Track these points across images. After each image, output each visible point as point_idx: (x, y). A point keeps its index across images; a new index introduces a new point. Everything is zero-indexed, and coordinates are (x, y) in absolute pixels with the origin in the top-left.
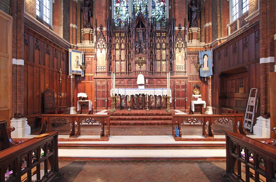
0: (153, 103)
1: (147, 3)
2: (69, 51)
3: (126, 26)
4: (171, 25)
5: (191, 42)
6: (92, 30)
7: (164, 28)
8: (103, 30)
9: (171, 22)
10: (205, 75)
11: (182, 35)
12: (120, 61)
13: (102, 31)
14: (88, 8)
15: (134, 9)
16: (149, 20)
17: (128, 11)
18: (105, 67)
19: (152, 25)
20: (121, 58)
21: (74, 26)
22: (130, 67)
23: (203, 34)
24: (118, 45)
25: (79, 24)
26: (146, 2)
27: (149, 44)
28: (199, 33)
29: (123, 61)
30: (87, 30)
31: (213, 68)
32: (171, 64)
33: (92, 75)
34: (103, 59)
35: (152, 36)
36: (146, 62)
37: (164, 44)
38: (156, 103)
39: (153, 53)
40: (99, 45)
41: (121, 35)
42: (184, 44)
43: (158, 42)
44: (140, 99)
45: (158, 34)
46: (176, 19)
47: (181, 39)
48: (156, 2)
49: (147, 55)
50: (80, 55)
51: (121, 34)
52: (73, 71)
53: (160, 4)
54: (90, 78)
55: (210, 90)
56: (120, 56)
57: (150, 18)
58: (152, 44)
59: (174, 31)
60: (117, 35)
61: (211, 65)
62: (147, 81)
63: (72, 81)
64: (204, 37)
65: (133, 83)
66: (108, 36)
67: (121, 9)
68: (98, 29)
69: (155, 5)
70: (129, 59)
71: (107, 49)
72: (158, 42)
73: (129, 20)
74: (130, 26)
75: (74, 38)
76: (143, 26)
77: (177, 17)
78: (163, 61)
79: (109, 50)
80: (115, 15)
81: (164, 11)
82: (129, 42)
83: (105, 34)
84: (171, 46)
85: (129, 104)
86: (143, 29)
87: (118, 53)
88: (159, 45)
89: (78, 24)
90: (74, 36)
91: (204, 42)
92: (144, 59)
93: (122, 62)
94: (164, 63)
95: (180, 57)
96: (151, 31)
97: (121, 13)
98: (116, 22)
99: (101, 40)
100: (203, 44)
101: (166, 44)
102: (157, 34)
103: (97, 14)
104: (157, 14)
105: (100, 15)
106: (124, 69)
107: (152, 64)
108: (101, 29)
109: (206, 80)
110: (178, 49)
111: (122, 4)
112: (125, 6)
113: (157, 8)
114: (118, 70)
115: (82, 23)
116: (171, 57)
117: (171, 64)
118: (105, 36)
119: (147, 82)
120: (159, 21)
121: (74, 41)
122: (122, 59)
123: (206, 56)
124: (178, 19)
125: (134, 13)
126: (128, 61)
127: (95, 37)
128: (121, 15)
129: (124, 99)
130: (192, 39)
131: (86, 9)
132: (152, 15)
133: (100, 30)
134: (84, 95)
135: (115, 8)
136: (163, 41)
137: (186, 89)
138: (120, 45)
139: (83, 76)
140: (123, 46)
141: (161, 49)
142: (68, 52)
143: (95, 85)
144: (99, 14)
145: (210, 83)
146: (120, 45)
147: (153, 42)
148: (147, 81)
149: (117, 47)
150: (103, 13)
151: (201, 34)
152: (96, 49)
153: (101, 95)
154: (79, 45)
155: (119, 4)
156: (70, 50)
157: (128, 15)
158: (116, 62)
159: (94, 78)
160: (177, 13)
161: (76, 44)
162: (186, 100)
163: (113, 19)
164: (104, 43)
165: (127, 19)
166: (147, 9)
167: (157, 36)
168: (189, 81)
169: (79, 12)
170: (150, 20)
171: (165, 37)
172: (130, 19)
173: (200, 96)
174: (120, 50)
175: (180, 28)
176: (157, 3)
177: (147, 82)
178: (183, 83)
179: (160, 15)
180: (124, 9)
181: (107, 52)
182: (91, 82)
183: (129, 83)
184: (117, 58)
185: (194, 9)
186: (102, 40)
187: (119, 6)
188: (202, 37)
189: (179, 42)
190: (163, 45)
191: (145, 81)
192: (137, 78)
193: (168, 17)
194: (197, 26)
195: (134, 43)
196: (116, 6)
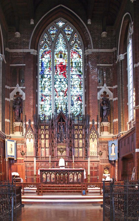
1: (67, 101)
2: (6, 140)
3: (49, 120)
4: (86, 120)
5: (103, 133)
6: (22, 123)
7: (81, 122)
8: (31, 124)
9: (86, 118)
10: (113, 159)
11: (94, 128)
12: (45, 148)
13: (30, 125)
14: (19, 106)
15: (56, 106)
16: (68, 116)
17: (51, 108)
18: (33, 153)
19: (71, 120)
20: (45, 146)
21: (8, 121)
22: (53, 153)
23: (112, 127)
24: (43, 135)
25: (11, 119)
26: (66, 101)
27: (68, 135)
28: (109, 126)
29: (48, 148)
30: (18, 124)
31: (118, 154)
32: (86, 150)
33: (23, 158)
34: (31, 147)
35: (71, 128)
36: (66, 149)
37: (81, 135)
38: (73, 179)
39: (72, 142)
40: (28, 136)
41: (46, 127)
42: (96, 136)
43: (76, 133)
44: (62, 177)
45: (76, 127)
46: (90, 116)
47: (94, 131)
48: (74, 101)
49: (67, 144)
50: (13, 143)
51: (46, 127)
52: (8, 156)
53: (78, 103)
54: (21, 161)
55: (116, 170)
56: (45, 144)
57: (69, 114)
58: (71, 135)
59: (88, 125)
60: (43, 127)
61: (117, 151)
62: (67, 163)
63: (7, 163)
64: (112, 130)
65: (55, 165)
66: (35, 128)
67: (45, 107)
68: (27, 123)
69: (73, 103)
70: (52, 147)
71: (34, 139)
72: (76, 133)
73: (52, 115)
74: (53, 120)
75: (8, 130)
76: (63, 121)
77: (91, 114)
78: (80, 148)
79: (36, 140)
80: (40, 111)
81: (81, 108)
82: (52, 133)
83: (32, 127)
84: (86, 137)
85: (52, 181)
86: (63, 123)
87: (43, 141)
88: (77, 135)
89: (10, 119)
90: (8, 128)
91: (112, 133)
92: (65, 147)
93: (46, 149)
94: (80, 149)
96: (70, 125)
97: (45, 109)
98: (41, 116)
99: (30, 131)
100: (112, 135)
101: (83, 135)
102: (75, 127)
103: (27, 111)
104: (75, 111)
105: (29, 112)
106: (48, 155)
107: (71, 151)
108: (30, 123)
109: (113, 163)
110: (91, 139)
111: (46, 102)
112: (49, 104)
113: (75, 106)
114: (43, 155)
115: (14, 118)
116: (86, 146)
117: (86, 150)
118: (33, 129)
119: (67, 165)
120: (78, 116)
121: (8, 132)
122: (47, 147)
123: (113, 145)
124: (92, 116)
125: (56, 111)
126: (52, 148)
127: (24, 130)
128: (46, 111)
129: (49, 177)
130: (103, 131)
131: (17, 107)
132: (71, 111)
133: (29, 124)
134: (16, 174)
135: (40, 105)
136: (80, 132)
137: (98, 169)
138: (45, 135)
139: (15, 159)
141: (78, 138)
142: (4, 141)
143: (25, 166)
144: (28, 111)
145: (117, 165)
146: (45, 135)
147: (72, 133)
148: (67, 163)
149: (43, 137)
150: (31, 110)
151: (110, 127)
152: (25, 138)
153: (30, 174)
154: (11, 135)
155: (43, 102)
156: (6, 140)
157: (51, 111)
158: (42, 149)
159: (25, 161)
160: (91, 111)
161: (9, 135)
162: (98, 178)
163: (39, 115)
164: (32, 134)
165: (51, 115)
166: (66, 108)
167: (75, 128)
168: (101, 164)
169: (11, 109)
170: (69, 116)
171: (82, 130)
172: (53, 115)
173: (109, 175)
174: (45, 139)
175: (93, 123)
176: (75, 101)
177: (67, 165)
179: (77, 112)
180: (48, 107)
181: (34, 141)
182: (22, 164)
183: (52, 165)
184: (43, 146)
185: (105, 108)
186: (31, 131)
187: (44, 104)
188: (111, 129)
189: (93, 134)
190: (80, 135)
191: (65, 164)
192: (59, 161)
193: (84, 113)
194: (108, 121)
195: (56, 134)
196: (41, 104)
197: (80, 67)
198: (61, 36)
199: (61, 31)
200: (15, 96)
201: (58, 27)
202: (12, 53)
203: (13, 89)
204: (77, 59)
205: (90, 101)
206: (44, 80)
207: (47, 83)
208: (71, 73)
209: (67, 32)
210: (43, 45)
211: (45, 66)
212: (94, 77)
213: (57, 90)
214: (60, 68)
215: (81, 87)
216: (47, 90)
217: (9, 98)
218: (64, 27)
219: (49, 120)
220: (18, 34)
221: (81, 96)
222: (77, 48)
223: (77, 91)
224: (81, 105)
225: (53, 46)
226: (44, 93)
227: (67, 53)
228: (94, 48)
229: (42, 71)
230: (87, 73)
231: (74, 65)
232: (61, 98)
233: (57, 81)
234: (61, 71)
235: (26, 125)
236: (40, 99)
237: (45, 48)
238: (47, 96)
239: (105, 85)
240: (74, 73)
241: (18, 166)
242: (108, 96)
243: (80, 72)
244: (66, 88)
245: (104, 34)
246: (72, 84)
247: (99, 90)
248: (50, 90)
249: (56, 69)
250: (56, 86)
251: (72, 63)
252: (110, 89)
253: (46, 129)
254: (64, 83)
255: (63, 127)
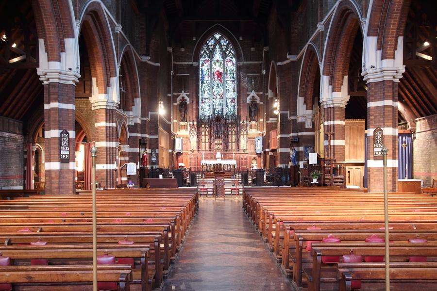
0: (226, 169)
10: (259, 152)
30: (183, 123)
45: (230, 125)
54: (186, 154)
59: (240, 124)
60: (203, 126)
61: (262, 146)
68: (191, 123)
77: (242, 116)
83: (195, 126)
84: (238, 134)
87: (203, 137)
95: (243, 141)
96: (225, 123)
97: (205, 110)
100: (259, 132)
101: (235, 132)
113: (230, 107)
116: (238, 141)
120: (231, 116)
125: (214, 113)
127: (189, 128)
128: (205, 111)
138: (205, 132)
140: (207, 133)
141: (232, 135)
146: (205, 132)
149: (203, 133)
154: (178, 133)
156: (175, 138)
157: (209, 111)
160: (242, 113)
171: (234, 127)
175: (243, 123)
178: (245, 157)
184: (203, 141)
185: (253, 110)
194: (255, 121)
197: (234, 74)
198: (218, 47)
199: (218, 42)
200: (180, 100)
201: (215, 38)
202: (178, 65)
203: (180, 95)
204: (231, 66)
205: (241, 105)
206: (204, 85)
207: (206, 88)
208: (226, 79)
209: (223, 44)
210: (202, 55)
211: (204, 73)
212: (245, 85)
213: (215, 94)
214: (217, 74)
215: (234, 91)
216: (206, 93)
217: (176, 102)
218: (220, 38)
219: (208, 119)
220: (183, 50)
221: (234, 99)
222: (231, 58)
223: (232, 94)
224: (234, 106)
225: (211, 55)
226: (204, 97)
227: (222, 62)
228: (244, 61)
229: (202, 77)
230: (239, 81)
231: (228, 72)
232: (218, 100)
233: (215, 86)
234: (218, 77)
235: (190, 124)
236: (201, 101)
237: (204, 58)
238: (206, 99)
239: (253, 91)
240: (229, 79)
241: (184, 158)
242: (256, 99)
243: (233, 78)
244: (222, 92)
245: (253, 49)
246: (227, 88)
247: (248, 95)
248: (209, 94)
249: (214, 76)
250: (213, 90)
251: (227, 70)
252: (257, 94)
253: (206, 127)
254: (221, 87)
255: (220, 127)
